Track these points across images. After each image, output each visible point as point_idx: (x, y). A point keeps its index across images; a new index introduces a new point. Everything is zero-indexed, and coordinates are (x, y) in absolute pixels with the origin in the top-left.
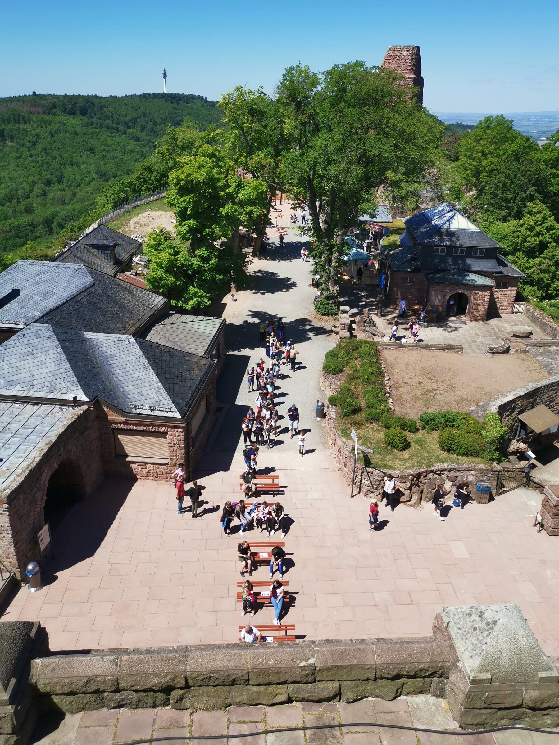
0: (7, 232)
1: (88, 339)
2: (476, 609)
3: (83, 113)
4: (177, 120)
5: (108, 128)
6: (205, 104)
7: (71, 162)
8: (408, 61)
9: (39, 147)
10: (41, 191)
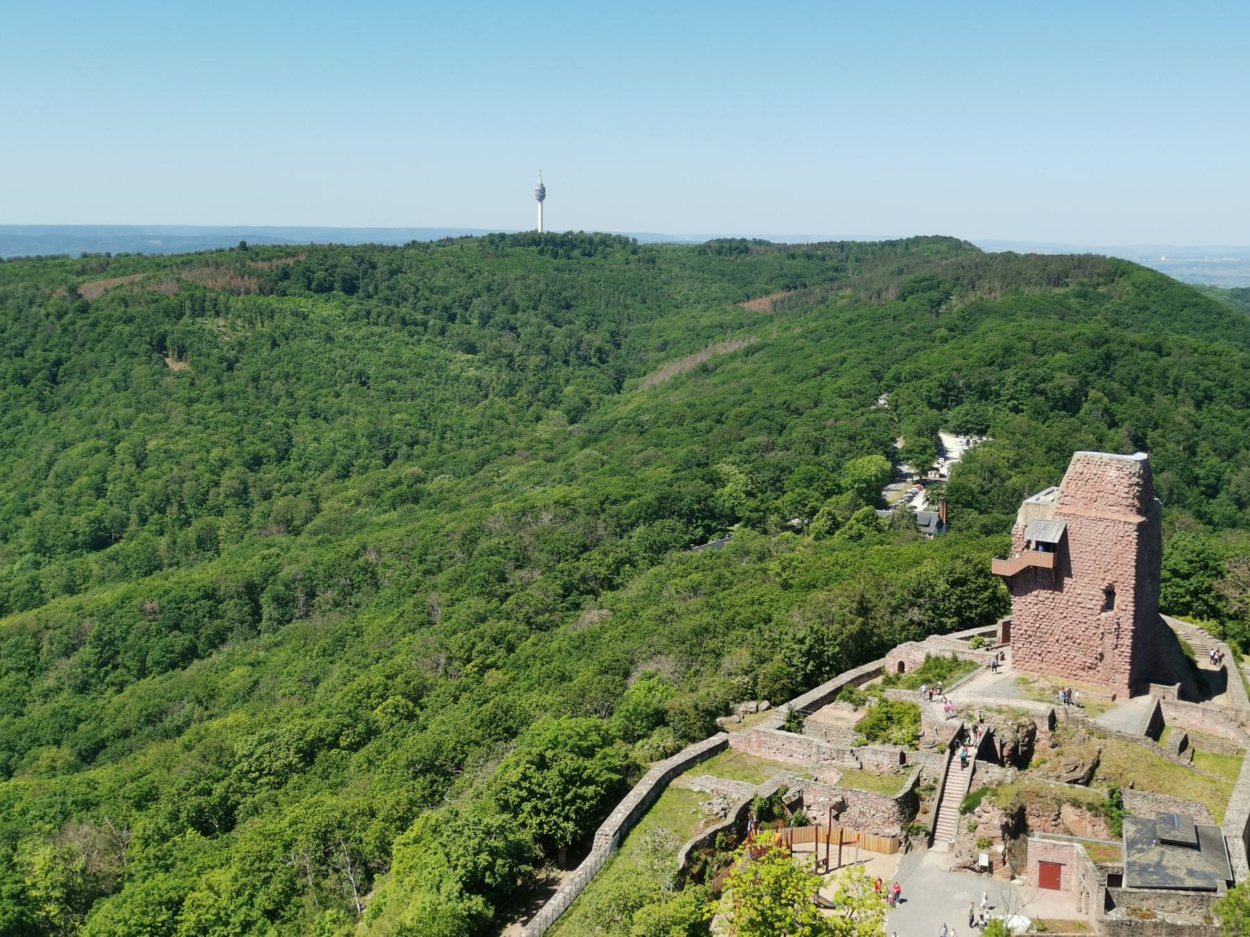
4: (564, 299)
5: (404, 322)
6: (632, 257)
7: (312, 408)
9: (243, 374)
10: (236, 483)
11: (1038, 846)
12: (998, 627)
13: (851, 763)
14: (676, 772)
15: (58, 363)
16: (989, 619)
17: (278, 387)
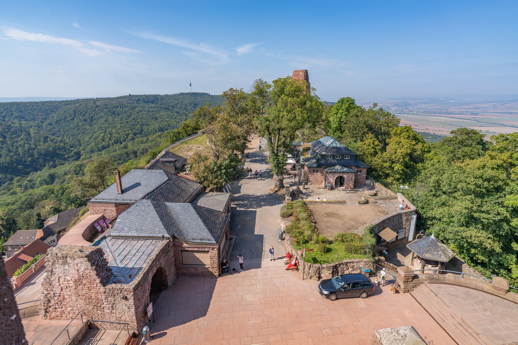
0: (115, 158)
1: (168, 206)
2: (394, 330)
3: (153, 102)
8: (303, 76)
9: (131, 118)
15: (93, 117)
17: (139, 120)
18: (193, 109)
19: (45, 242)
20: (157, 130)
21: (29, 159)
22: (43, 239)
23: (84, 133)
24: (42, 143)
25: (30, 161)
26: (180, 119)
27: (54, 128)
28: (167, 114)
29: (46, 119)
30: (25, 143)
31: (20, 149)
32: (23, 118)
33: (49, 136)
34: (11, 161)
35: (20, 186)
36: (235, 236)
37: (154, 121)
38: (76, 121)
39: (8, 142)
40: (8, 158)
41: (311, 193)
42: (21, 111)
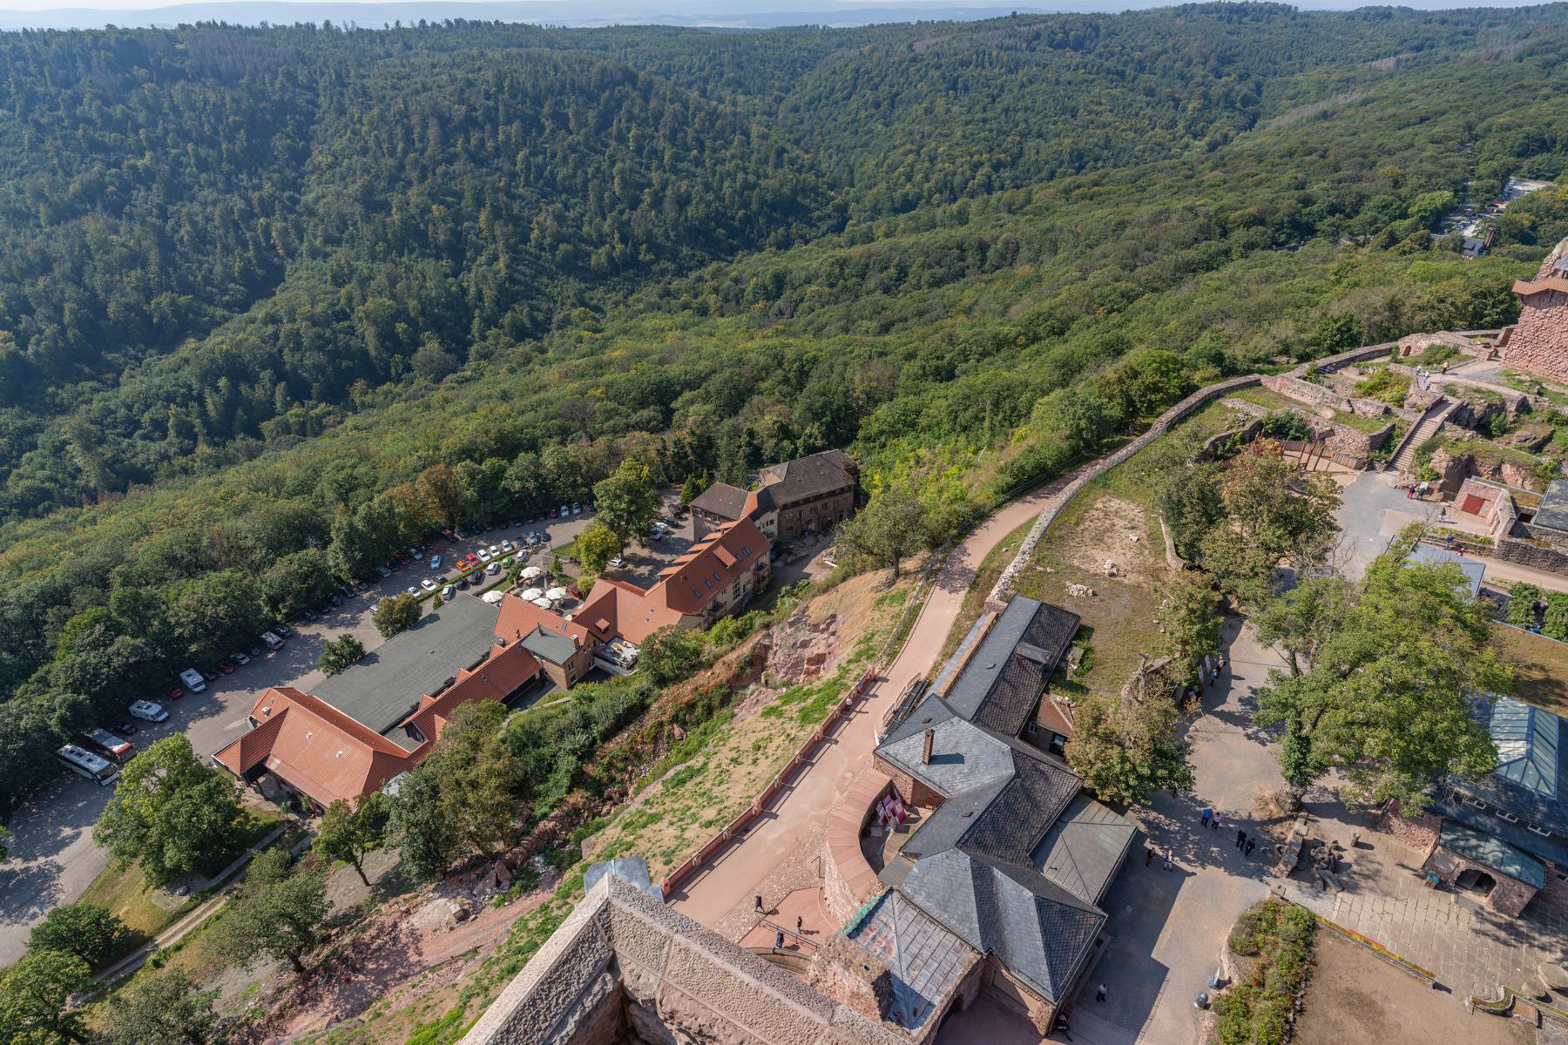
0: (927, 255)
3: (1078, 45)
9: (999, 107)
11: (1470, 486)
12: (1502, 332)
13: (1345, 407)
14: (1218, 395)
15: (898, 94)
16: (1496, 325)
18: (1211, 78)
19: (757, 523)
20: (1066, 157)
21: (741, 213)
22: (754, 516)
23: (866, 145)
24: (770, 170)
25: (740, 220)
26: (1151, 118)
27: (802, 122)
28: (1113, 98)
29: (788, 90)
30: (737, 166)
31: (726, 184)
32: (741, 85)
33: (788, 146)
34: (707, 216)
35: (716, 290)
36: (1109, 938)
37: (1066, 122)
38: (853, 105)
39: (708, 164)
40: (702, 206)
41: (1367, 877)
42: (740, 66)
